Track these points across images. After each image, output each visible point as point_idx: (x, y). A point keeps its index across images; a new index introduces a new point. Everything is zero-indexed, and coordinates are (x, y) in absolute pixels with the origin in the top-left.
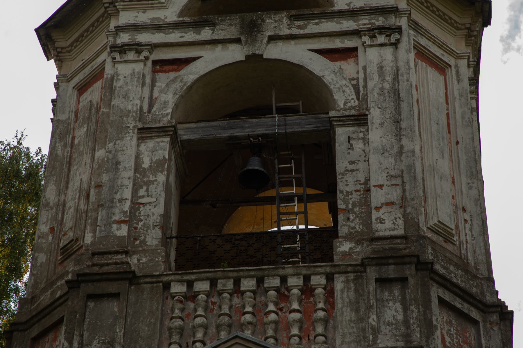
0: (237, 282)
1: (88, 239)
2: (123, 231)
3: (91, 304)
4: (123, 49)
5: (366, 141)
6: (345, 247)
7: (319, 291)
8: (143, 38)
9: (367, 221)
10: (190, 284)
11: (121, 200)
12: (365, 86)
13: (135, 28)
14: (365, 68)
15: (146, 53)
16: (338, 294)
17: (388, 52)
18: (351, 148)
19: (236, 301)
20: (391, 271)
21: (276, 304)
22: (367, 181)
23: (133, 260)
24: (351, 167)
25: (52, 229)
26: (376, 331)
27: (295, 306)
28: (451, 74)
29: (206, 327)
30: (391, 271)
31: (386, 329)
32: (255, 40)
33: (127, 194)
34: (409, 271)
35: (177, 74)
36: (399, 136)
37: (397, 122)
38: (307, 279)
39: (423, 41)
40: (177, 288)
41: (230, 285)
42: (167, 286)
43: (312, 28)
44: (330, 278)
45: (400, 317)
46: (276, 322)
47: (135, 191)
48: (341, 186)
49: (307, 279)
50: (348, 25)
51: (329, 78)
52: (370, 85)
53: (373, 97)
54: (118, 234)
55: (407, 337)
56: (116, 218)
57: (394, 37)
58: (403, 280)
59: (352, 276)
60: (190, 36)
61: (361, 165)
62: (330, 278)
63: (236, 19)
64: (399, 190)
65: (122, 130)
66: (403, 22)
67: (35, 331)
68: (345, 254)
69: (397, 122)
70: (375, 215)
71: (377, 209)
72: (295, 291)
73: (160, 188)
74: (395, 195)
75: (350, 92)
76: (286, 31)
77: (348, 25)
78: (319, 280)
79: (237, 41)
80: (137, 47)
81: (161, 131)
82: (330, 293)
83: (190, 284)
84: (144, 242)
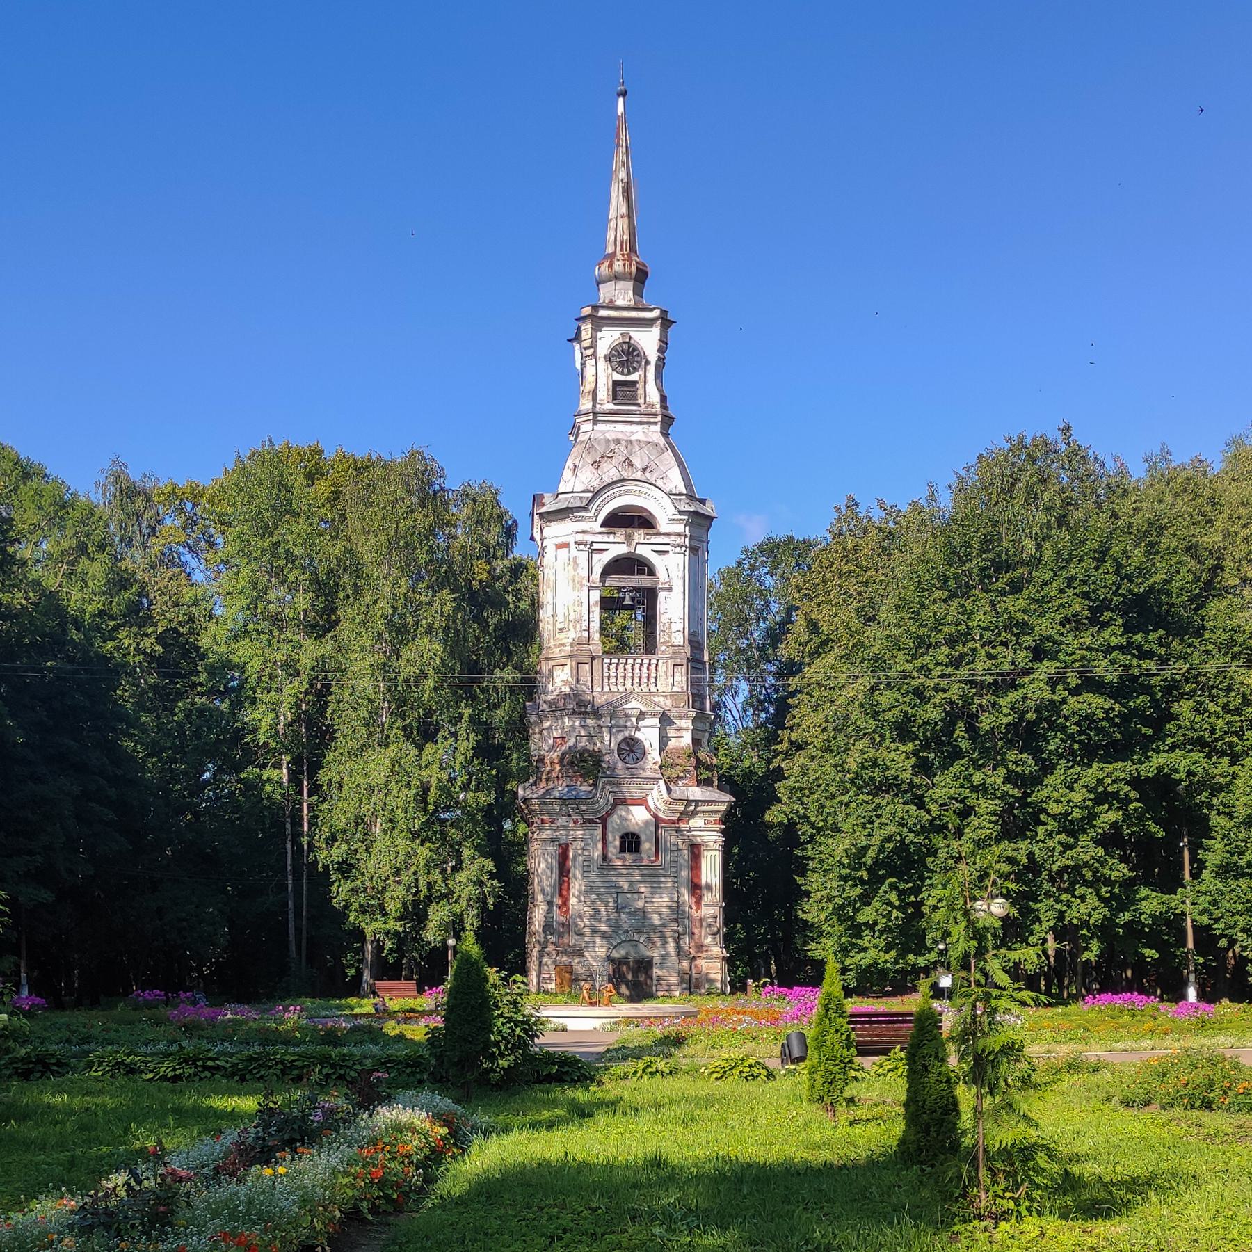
6: (663, 648)
9: (670, 637)
20: (678, 661)
23: (591, 647)
30: (678, 661)
40: (607, 661)
50: (666, 540)
60: (605, 539)
65: (582, 585)
67: (554, 663)
70: (673, 635)
77: (666, 540)
78: (654, 661)
82: (657, 665)
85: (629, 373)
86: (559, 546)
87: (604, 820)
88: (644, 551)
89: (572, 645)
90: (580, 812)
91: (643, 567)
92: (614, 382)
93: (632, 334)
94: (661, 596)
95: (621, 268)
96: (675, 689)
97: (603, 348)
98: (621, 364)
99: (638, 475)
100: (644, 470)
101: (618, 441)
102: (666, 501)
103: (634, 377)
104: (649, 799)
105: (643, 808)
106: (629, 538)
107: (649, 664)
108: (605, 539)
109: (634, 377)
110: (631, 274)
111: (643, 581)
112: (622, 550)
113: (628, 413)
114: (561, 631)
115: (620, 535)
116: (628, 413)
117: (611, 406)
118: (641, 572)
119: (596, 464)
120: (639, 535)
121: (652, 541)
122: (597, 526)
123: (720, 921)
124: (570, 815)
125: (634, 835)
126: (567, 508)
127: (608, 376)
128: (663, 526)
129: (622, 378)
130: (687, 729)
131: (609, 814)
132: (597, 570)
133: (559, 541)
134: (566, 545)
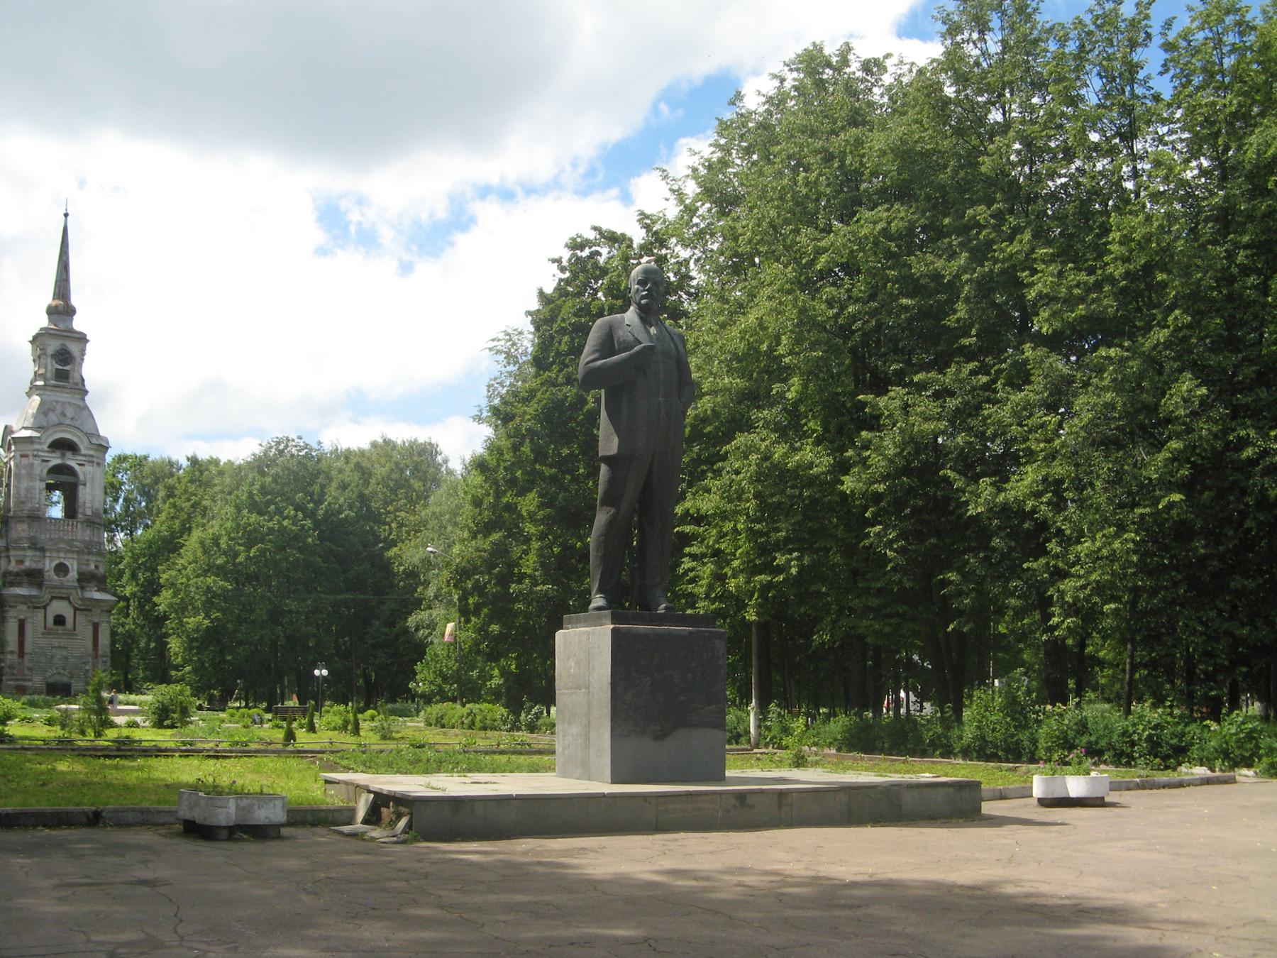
4: (35, 456)
13: (38, 450)
66: (95, 460)
80: (39, 456)
86: (22, 456)
87: (45, 608)
88: (73, 464)
91: (70, 471)
94: (81, 487)
97: (50, 350)
98: (61, 361)
99: (68, 422)
100: (72, 419)
101: (57, 402)
102: (85, 439)
105: (64, 604)
106: (63, 455)
111: (69, 479)
112: (58, 461)
113: (64, 387)
114: (22, 502)
115: (58, 454)
116: (64, 387)
117: (53, 382)
118: (68, 474)
119: (45, 414)
120: (69, 454)
122: (45, 447)
126: (31, 438)
128: (83, 451)
131: (47, 604)
132: (45, 471)
133: (23, 453)
134: (26, 456)
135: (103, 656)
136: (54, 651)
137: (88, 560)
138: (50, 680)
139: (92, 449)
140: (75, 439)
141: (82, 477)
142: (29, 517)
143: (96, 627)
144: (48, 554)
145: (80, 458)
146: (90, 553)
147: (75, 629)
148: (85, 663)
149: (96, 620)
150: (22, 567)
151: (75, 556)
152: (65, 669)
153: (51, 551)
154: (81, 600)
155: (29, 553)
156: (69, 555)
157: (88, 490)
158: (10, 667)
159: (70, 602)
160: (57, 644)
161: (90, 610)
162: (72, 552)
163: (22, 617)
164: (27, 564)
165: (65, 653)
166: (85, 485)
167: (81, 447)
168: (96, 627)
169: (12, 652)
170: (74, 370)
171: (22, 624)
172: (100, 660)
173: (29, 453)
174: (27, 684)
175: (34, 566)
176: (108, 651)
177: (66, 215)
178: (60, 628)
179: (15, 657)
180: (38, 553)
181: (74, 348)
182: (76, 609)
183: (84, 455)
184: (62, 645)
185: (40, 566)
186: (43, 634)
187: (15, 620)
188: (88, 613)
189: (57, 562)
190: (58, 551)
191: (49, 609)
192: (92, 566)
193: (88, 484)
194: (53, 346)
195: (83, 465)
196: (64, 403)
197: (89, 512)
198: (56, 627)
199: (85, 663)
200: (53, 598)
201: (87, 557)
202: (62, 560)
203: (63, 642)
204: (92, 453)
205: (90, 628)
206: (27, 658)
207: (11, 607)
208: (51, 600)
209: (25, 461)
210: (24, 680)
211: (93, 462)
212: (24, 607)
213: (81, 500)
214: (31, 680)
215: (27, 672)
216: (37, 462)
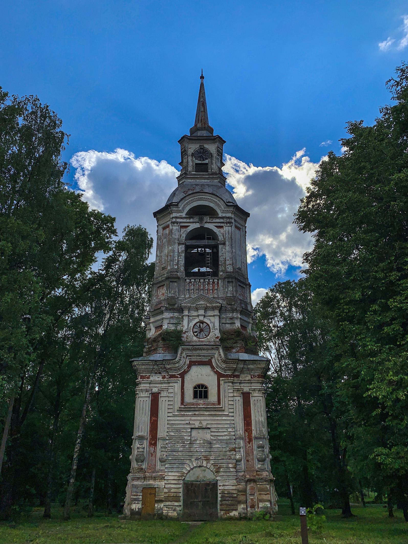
0: (200, 280)
1: (169, 268)
2: (176, 267)
3: (171, 283)
4: (174, 223)
5: (225, 249)
7: (216, 283)
8: (178, 220)
9: (225, 268)
10: (190, 280)
11: (175, 260)
12: (225, 236)
13: (176, 218)
14: (225, 231)
15: (179, 224)
16: (220, 284)
17: (230, 227)
18: (222, 250)
19: (199, 284)
20: (230, 280)
21: (207, 285)
22: (225, 258)
24: (222, 255)
25: (159, 262)
26: (227, 293)
27: (211, 286)
28: (241, 230)
29: (193, 289)
30: (230, 280)
31: (229, 292)
32: (202, 223)
33: (177, 259)
34: (234, 280)
35: (186, 229)
36: (232, 248)
37: (232, 245)
38: (214, 280)
39: (237, 224)
40: (188, 281)
41: (198, 281)
42: (186, 280)
43: (214, 221)
44: (218, 280)
45: (232, 290)
46: (207, 289)
47: (178, 258)
48: (220, 259)
49: (214, 280)
50: (222, 220)
51: (218, 233)
52: (226, 236)
53: (227, 239)
54: (175, 268)
55: (233, 294)
56: (174, 264)
57: (231, 224)
58: (232, 282)
59: (222, 280)
60: (188, 221)
61: (224, 255)
62: (218, 280)
63: (198, 217)
64: (232, 261)
65: (175, 243)
66: (233, 221)
68: (221, 275)
69: (232, 245)
71: (227, 265)
72: (211, 283)
73: (183, 257)
74: (231, 262)
75: (222, 236)
76: (209, 221)
77: (222, 220)
78: (216, 281)
79: (198, 222)
80: (177, 223)
81: (183, 244)
82: (218, 283)
83: (190, 280)
84: (180, 269)
85: (204, 160)
86: (164, 228)
87: (182, 376)
88: (211, 226)
89: (167, 273)
90: (166, 370)
92: (196, 164)
93: (206, 146)
95: (201, 126)
96: (229, 295)
97: (190, 151)
101: (197, 185)
102: (221, 203)
103: (206, 161)
104: (213, 361)
107: (213, 282)
108: (188, 221)
109: (206, 161)
110: (205, 127)
111: (212, 242)
112: (197, 225)
114: (163, 268)
115: (196, 219)
118: (209, 239)
120: (207, 219)
121: (214, 221)
122: (184, 215)
123: (267, 450)
124: (160, 373)
125: (203, 386)
127: (193, 161)
128: (220, 215)
129: (200, 162)
130: (237, 318)
131: (185, 372)
132: (184, 235)
134: (168, 226)
135: (256, 438)
136: (194, 433)
137: (231, 319)
138: (188, 478)
139: (228, 212)
140: (212, 205)
141: (221, 238)
142: (167, 278)
143: (246, 397)
144: (186, 313)
145: (218, 220)
146: (233, 311)
147: (219, 403)
148: (234, 450)
149: (246, 389)
150: (159, 332)
151: (217, 312)
152: (208, 460)
153: (189, 309)
154: (225, 362)
155: (167, 315)
156: (210, 313)
157: (227, 248)
158: (137, 461)
159: (213, 368)
160: (197, 425)
161: (238, 376)
162: (213, 309)
163: (155, 390)
164: (165, 327)
165: (208, 436)
166: (224, 244)
167: (219, 211)
168: (246, 397)
169: (141, 438)
170: (212, 164)
171: (155, 398)
172: (255, 444)
173: (168, 223)
174: (157, 483)
175: (172, 328)
176: (265, 431)
177: (202, 77)
178: (201, 401)
179: (146, 443)
180: (176, 315)
181: (212, 148)
182: (219, 375)
183: (223, 218)
184: (204, 424)
185: (179, 328)
186: (180, 410)
187: (147, 394)
188: (236, 380)
189: (197, 320)
190: (197, 309)
191: (187, 378)
192: (238, 324)
193: (227, 243)
194: (193, 148)
195: (222, 227)
196: (202, 185)
197: (230, 269)
198: (195, 400)
199: (234, 450)
200: (192, 364)
201: (230, 315)
202: (201, 318)
203: (206, 420)
204: (229, 215)
205: (239, 400)
206: (160, 444)
207: (142, 377)
208: (189, 367)
209: (167, 231)
210: (155, 479)
211: (230, 223)
212: (157, 378)
213: (221, 259)
214: (163, 478)
215: (159, 466)
216: (175, 228)
